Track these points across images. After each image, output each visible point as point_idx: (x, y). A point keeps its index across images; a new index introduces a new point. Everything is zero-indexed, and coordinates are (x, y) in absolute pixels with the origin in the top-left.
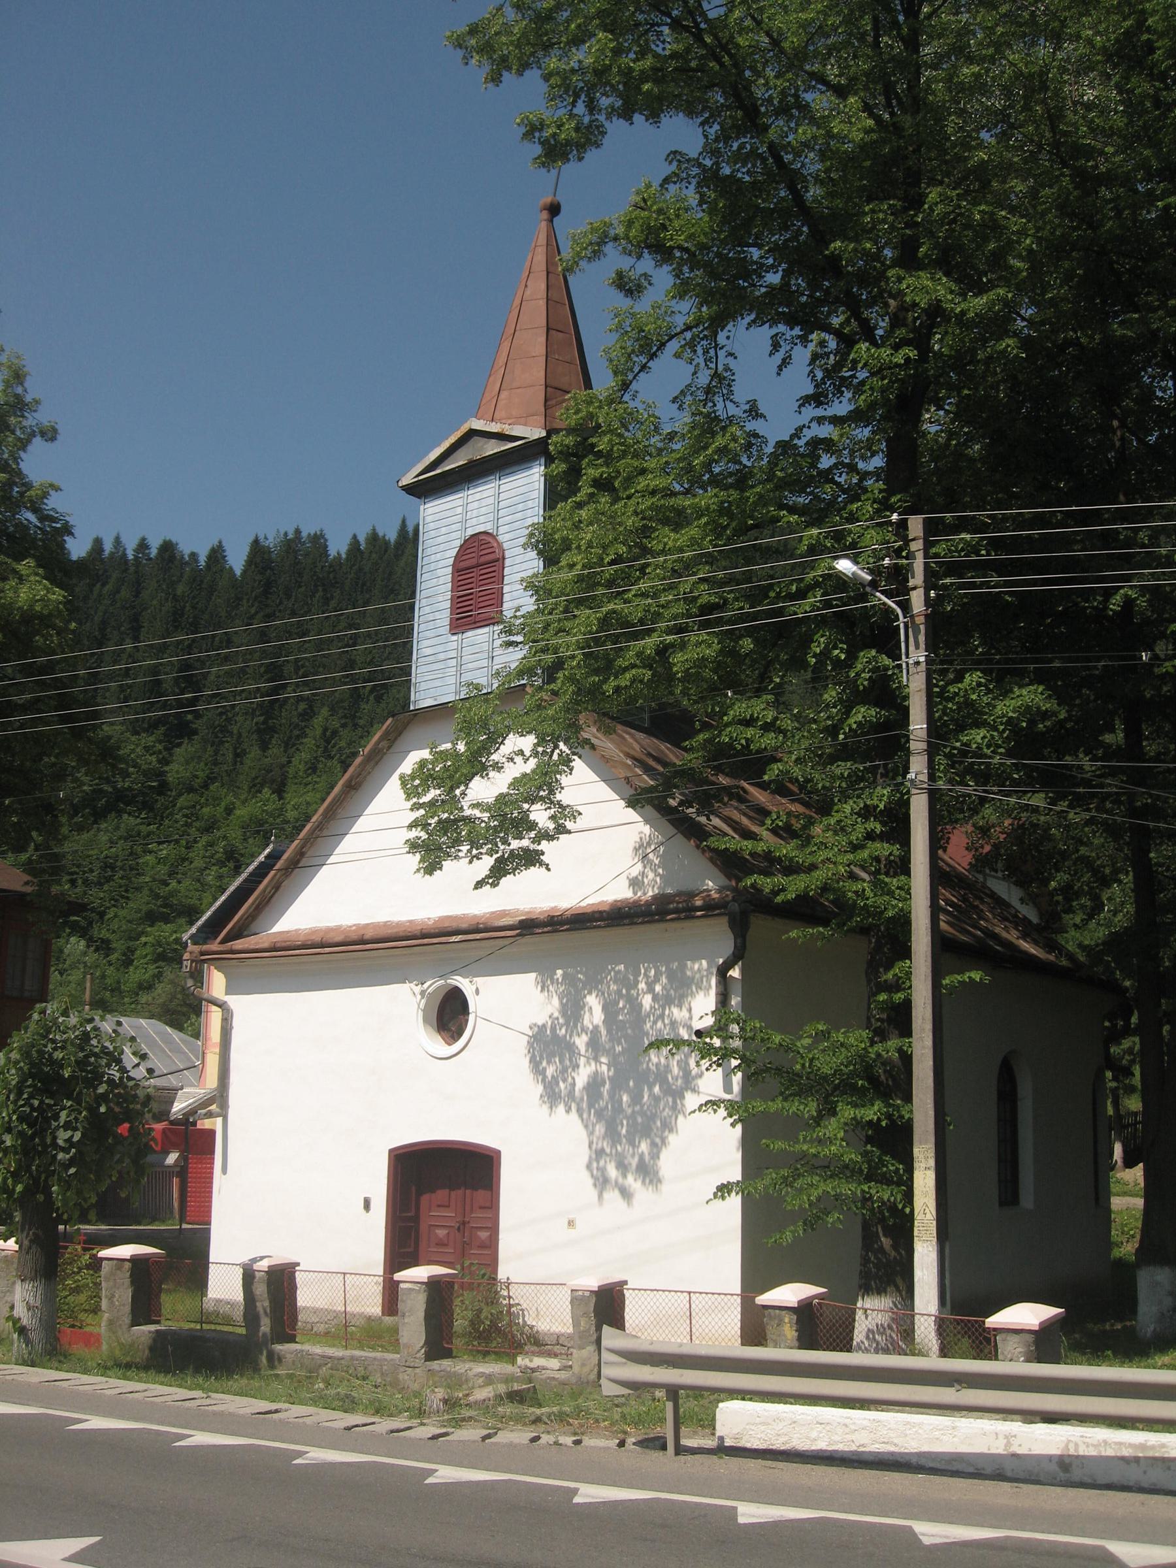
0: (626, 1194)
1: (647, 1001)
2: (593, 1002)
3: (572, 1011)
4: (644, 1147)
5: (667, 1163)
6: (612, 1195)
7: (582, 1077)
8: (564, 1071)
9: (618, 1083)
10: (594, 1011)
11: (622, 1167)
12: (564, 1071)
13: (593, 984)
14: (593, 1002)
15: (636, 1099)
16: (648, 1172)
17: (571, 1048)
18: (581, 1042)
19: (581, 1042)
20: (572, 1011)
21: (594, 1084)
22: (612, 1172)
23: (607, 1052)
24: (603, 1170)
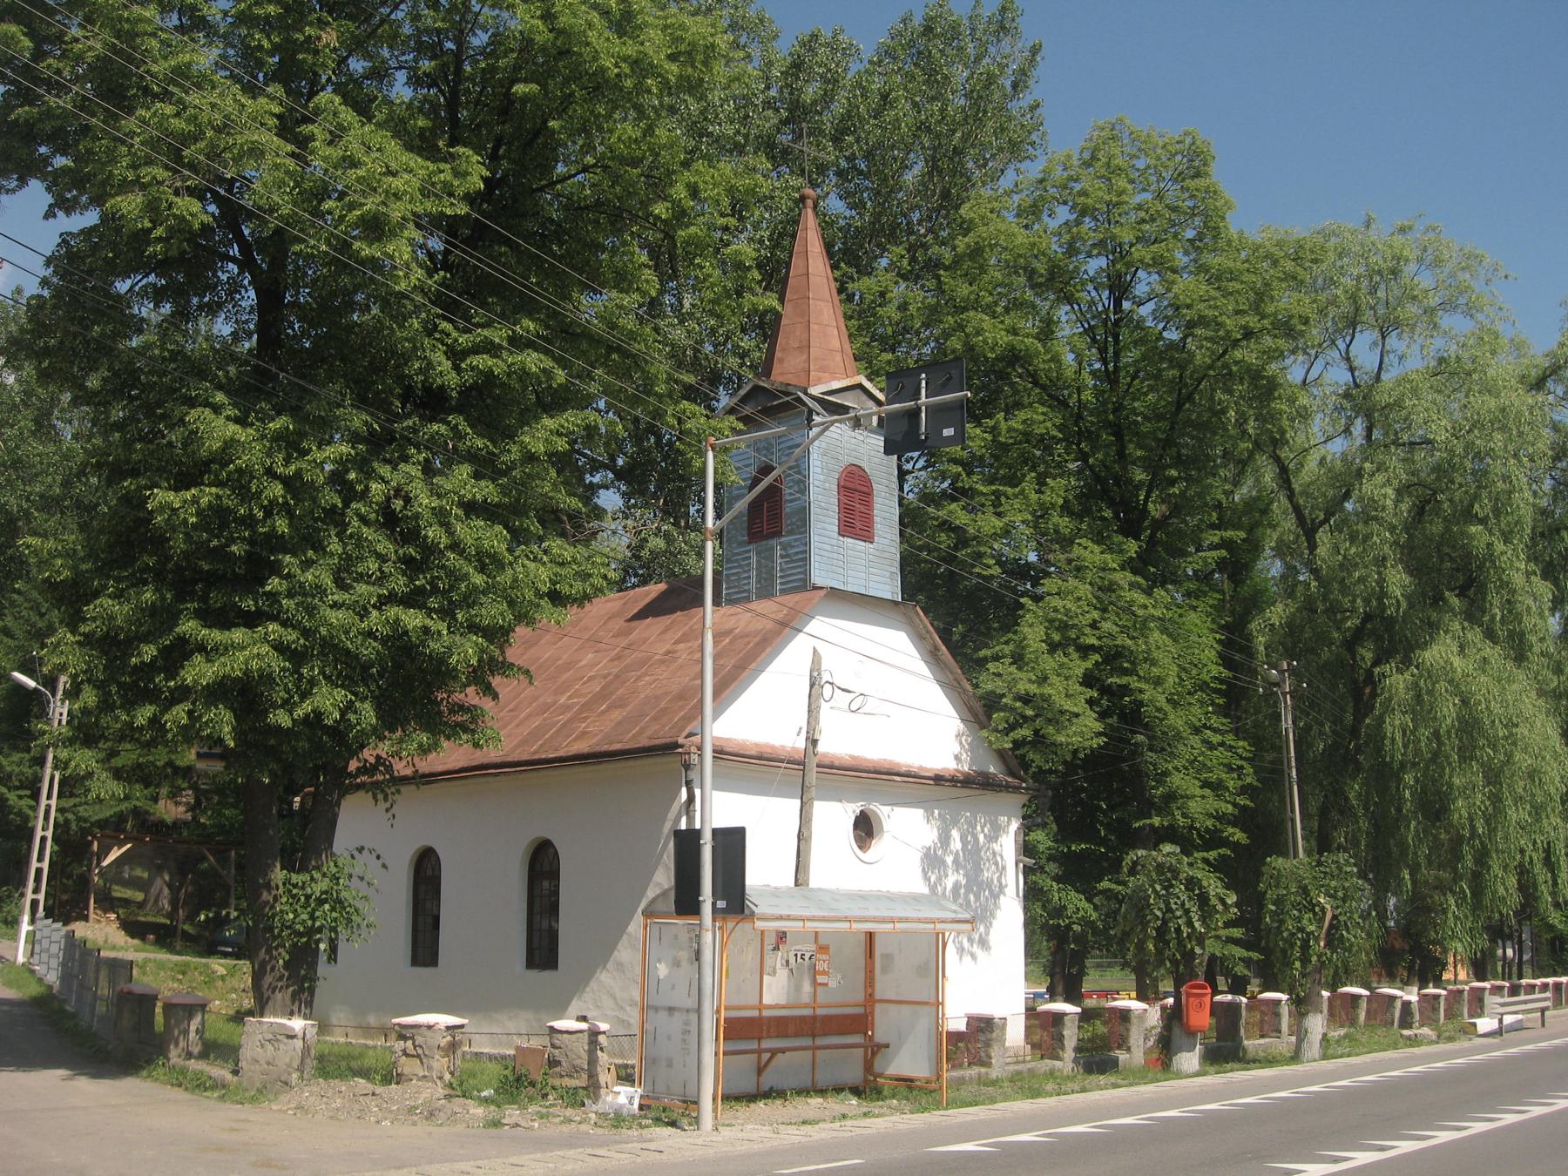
0: (973, 956)
1: (981, 837)
2: (955, 834)
3: (945, 839)
4: (982, 929)
5: (993, 938)
6: (967, 958)
7: (949, 883)
8: (939, 879)
9: (968, 889)
10: (956, 845)
11: (970, 940)
12: (939, 879)
13: (955, 822)
14: (955, 834)
15: (977, 898)
16: (984, 943)
17: (944, 862)
18: (949, 860)
19: (949, 860)
20: (945, 839)
21: (957, 886)
22: (966, 944)
23: (964, 868)
24: (961, 943)
